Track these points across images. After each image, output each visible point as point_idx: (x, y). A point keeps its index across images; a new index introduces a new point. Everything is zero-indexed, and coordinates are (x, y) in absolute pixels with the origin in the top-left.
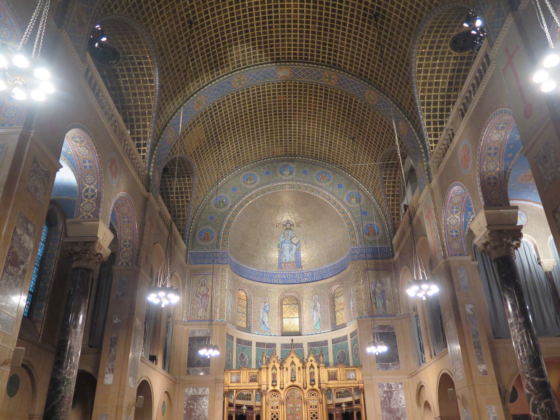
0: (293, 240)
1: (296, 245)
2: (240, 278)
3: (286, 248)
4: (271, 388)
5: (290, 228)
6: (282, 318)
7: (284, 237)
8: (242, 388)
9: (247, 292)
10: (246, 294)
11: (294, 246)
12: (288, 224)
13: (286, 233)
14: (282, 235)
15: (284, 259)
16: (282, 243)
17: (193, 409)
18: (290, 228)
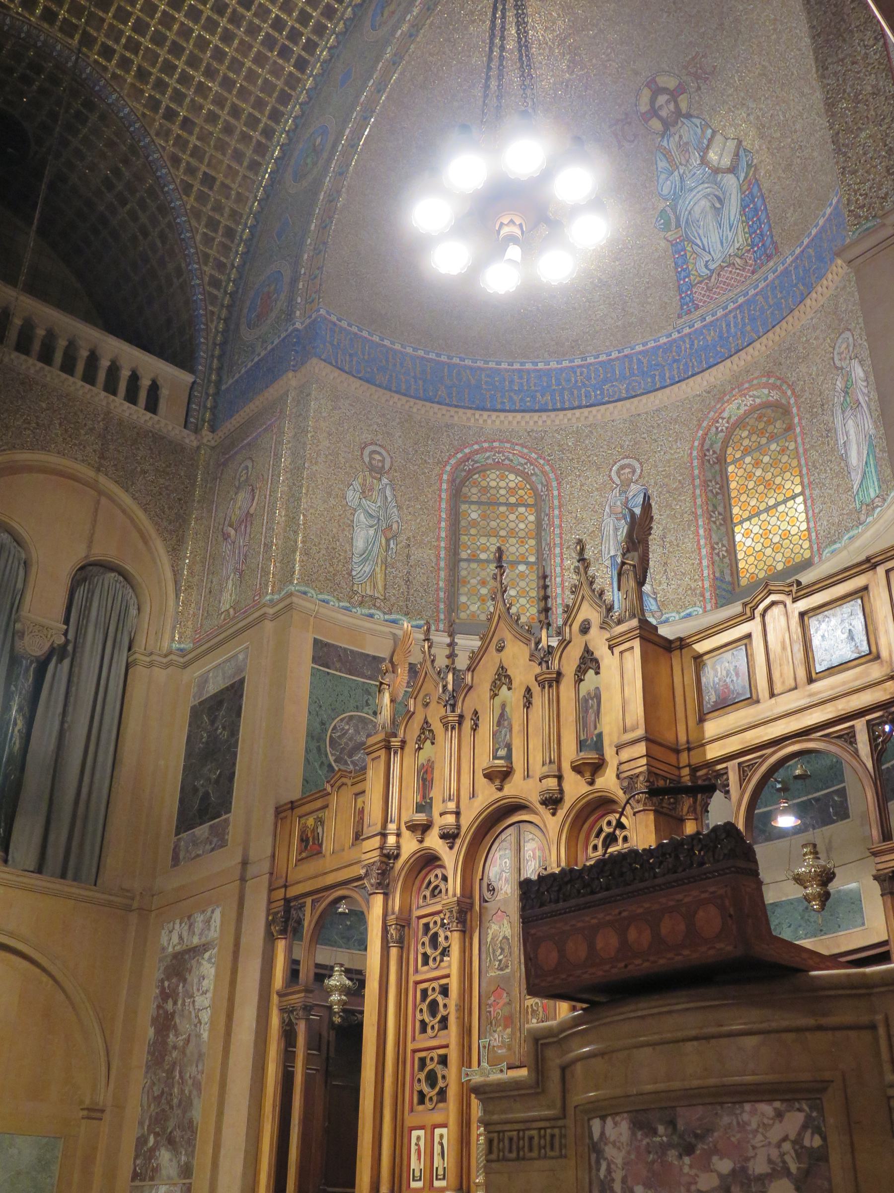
0: (712, 156)
1: (732, 170)
2: (437, 413)
3: (697, 210)
4: (409, 846)
5: (678, 113)
6: (727, 524)
7: (674, 165)
8: (330, 880)
9: (529, 469)
10: (526, 476)
11: (730, 182)
12: (662, 99)
13: (671, 144)
14: (662, 164)
15: (701, 264)
16: (676, 198)
17: (173, 1014)
18: (678, 113)
